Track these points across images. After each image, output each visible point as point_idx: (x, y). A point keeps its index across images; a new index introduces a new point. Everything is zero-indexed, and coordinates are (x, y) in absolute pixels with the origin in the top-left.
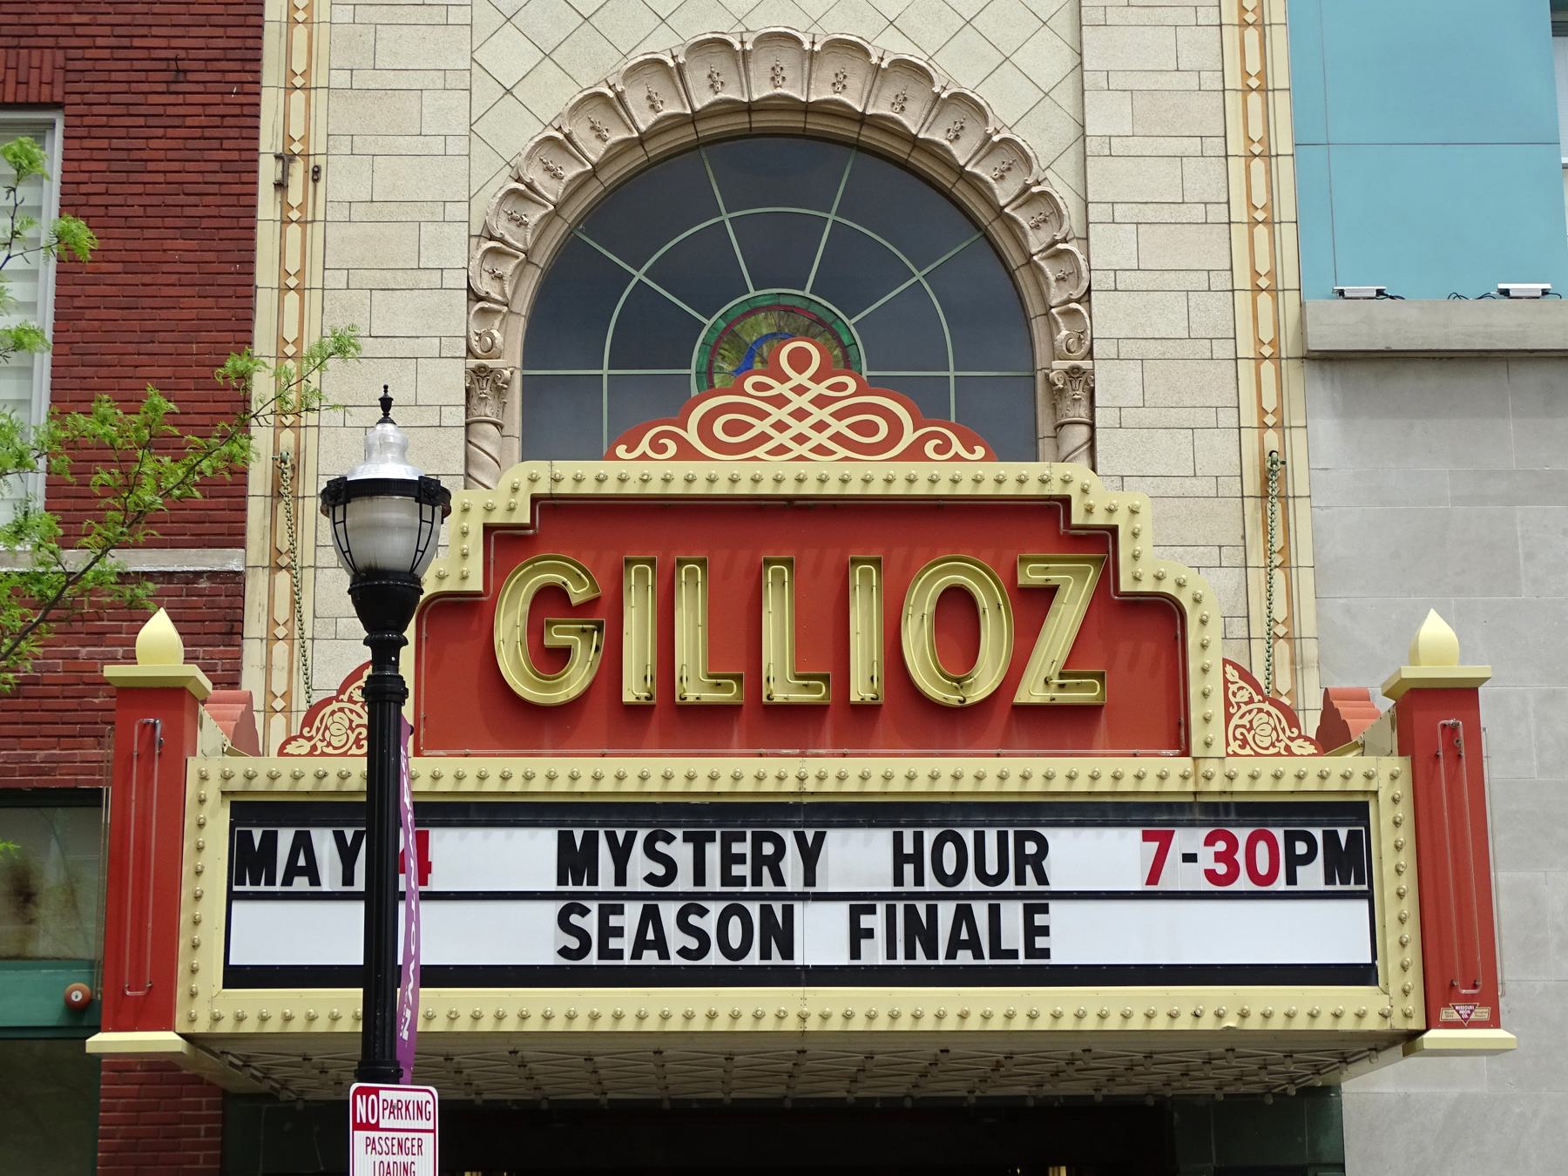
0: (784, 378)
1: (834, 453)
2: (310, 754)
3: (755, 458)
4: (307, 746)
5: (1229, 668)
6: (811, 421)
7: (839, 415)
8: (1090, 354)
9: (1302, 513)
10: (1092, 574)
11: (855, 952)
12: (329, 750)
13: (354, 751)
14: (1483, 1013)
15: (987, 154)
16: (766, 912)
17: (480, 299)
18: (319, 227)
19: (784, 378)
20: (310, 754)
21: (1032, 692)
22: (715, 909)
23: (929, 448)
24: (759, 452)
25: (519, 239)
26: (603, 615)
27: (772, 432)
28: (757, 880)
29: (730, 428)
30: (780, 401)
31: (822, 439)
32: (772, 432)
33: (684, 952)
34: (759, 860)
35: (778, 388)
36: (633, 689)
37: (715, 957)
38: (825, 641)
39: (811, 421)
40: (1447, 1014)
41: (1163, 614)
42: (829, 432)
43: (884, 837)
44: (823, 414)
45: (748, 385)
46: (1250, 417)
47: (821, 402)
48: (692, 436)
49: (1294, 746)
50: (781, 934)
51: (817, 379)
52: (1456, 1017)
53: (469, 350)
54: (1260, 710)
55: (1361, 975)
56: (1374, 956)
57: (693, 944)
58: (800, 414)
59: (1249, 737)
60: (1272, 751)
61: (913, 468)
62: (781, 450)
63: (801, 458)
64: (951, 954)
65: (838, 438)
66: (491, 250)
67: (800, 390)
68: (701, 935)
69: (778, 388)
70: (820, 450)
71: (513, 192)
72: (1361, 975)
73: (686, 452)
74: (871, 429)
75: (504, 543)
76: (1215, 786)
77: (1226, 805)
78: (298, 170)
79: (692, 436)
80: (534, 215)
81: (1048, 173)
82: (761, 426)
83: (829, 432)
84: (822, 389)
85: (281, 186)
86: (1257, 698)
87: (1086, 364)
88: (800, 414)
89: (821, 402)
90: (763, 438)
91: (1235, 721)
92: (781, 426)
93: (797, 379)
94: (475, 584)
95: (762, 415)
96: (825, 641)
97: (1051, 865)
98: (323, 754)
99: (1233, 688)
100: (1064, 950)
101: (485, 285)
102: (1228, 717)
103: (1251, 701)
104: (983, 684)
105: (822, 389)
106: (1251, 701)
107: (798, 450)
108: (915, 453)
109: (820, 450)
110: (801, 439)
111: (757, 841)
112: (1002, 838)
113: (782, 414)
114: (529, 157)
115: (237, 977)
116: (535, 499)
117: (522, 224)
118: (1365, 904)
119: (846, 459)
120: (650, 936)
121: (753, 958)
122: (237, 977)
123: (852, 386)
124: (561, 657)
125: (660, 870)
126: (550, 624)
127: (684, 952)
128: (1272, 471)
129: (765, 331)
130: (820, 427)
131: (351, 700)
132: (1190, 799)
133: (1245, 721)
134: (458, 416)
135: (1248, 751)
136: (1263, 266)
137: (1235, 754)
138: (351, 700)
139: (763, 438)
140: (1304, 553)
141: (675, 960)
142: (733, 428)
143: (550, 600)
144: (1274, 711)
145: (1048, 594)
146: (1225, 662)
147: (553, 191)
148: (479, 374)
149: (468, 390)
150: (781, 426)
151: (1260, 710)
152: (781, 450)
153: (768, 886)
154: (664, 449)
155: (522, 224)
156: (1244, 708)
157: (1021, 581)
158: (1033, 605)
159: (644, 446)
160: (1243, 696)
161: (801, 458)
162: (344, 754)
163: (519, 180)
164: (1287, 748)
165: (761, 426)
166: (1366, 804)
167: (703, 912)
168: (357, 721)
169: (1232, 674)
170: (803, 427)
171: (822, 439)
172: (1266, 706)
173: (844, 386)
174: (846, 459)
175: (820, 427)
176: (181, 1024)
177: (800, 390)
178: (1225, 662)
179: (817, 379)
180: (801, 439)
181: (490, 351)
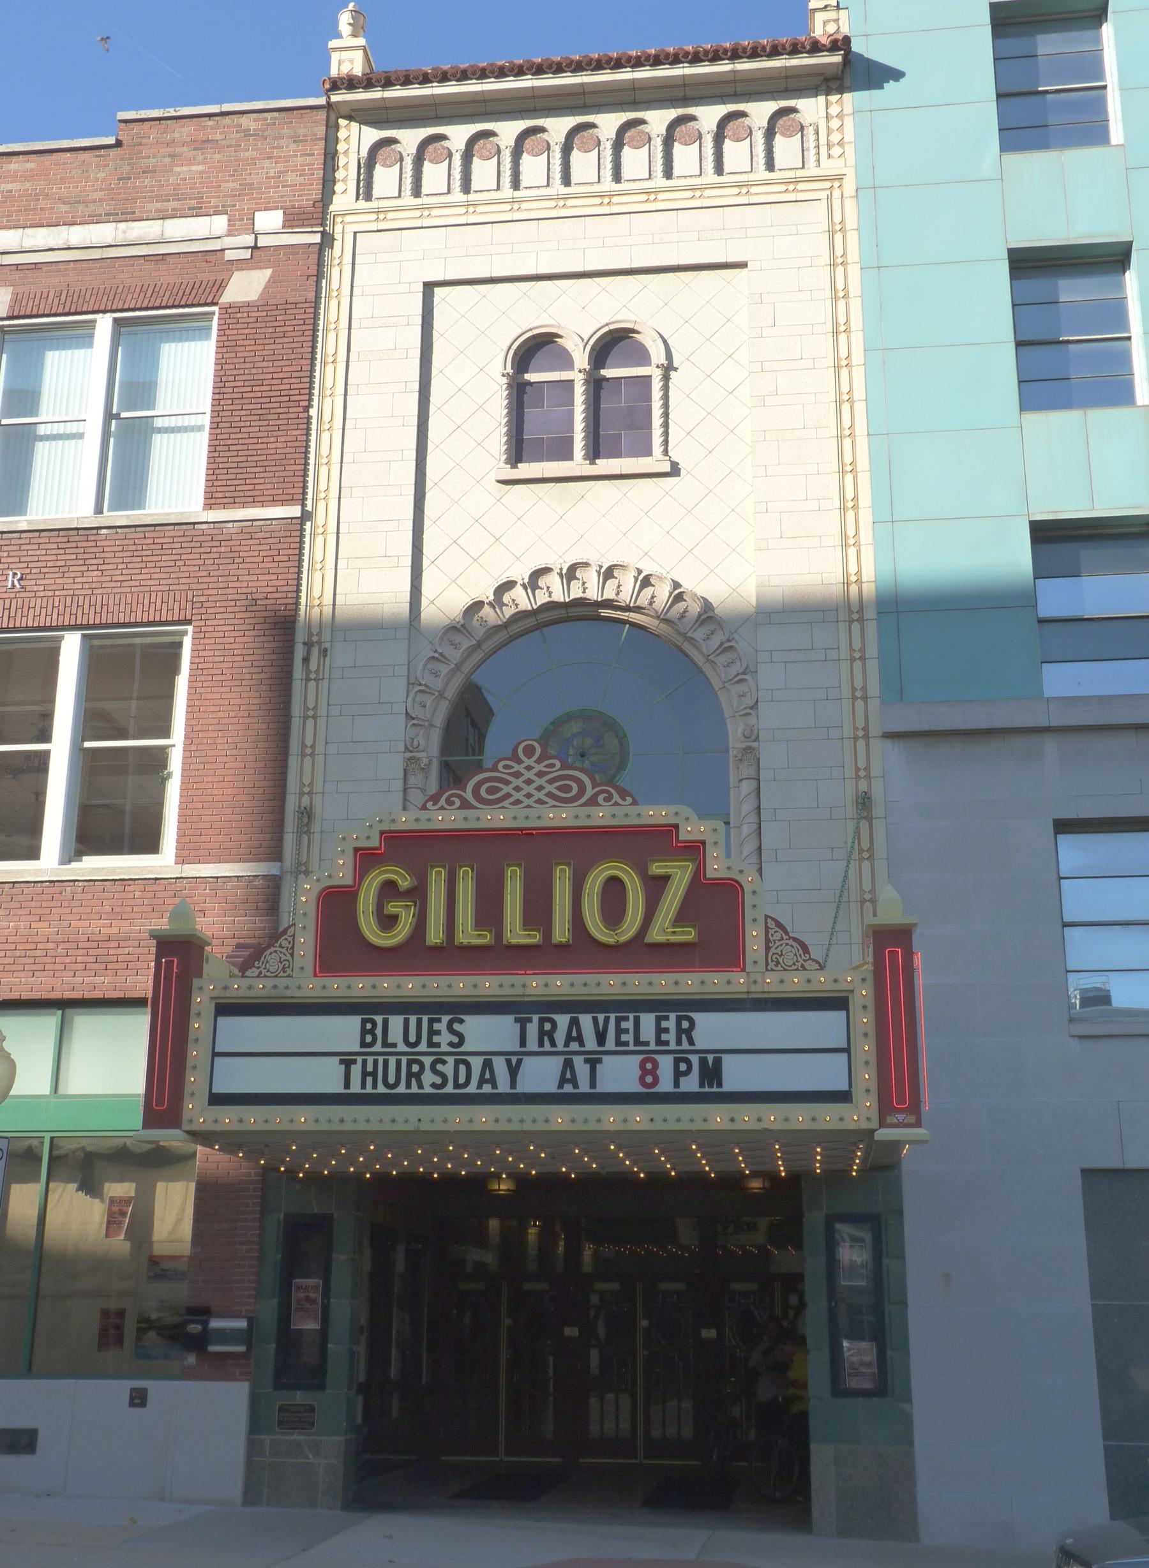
0: (520, 762)
1: (546, 803)
2: (258, 976)
3: (503, 807)
4: (257, 972)
5: (769, 920)
6: (535, 785)
7: (550, 782)
8: (757, 738)
9: (880, 827)
10: (691, 867)
11: (677, 1084)
12: (269, 974)
13: (282, 974)
14: (912, 1119)
15: (700, 625)
16: (703, 1062)
17: (413, 719)
18: (326, 682)
19: (520, 762)
20: (258, 976)
21: (656, 935)
22: (451, 1060)
23: (600, 799)
24: (506, 803)
25: (438, 683)
26: (418, 894)
27: (513, 792)
28: (679, 1042)
29: (490, 791)
30: (517, 775)
31: (541, 795)
32: (513, 792)
33: (433, 1085)
34: (680, 1031)
35: (517, 768)
36: (435, 935)
37: (449, 1089)
38: (537, 910)
39: (535, 785)
40: (889, 1120)
41: (730, 889)
43: (355, 1021)
44: (542, 782)
45: (500, 766)
46: (850, 772)
47: (540, 774)
48: (468, 795)
49: (806, 965)
50: (712, 1073)
51: (538, 761)
52: (895, 1121)
53: (406, 748)
54: (787, 944)
55: (844, 1097)
56: (850, 1086)
57: (439, 1081)
58: (529, 782)
59: (781, 960)
60: (794, 967)
61: (591, 810)
62: (517, 802)
63: (529, 806)
64: (480, 1086)
65: (550, 795)
66: (420, 691)
67: (529, 768)
68: (443, 1076)
69: (517, 768)
70: (540, 802)
71: (433, 658)
72: (844, 1097)
73: (465, 805)
74: (568, 789)
75: (366, 859)
76: (758, 988)
77: (766, 999)
78: (315, 651)
79: (468, 795)
80: (444, 669)
81: (736, 636)
82: (507, 789)
83: (545, 791)
84: (539, 768)
85: (306, 660)
86: (785, 937)
87: (755, 745)
88: (529, 782)
89: (540, 774)
90: (508, 795)
91: (773, 951)
92: (518, 789)
93: (528, 762)
94: (348, 881)
95: (507, 783)
96: (537, 910)
97: (695, 1034)
98: (265, 976)
99: (771, 932)
100: (731, 1082)
101: (416, 711)
102: (768, 949)
103: (782, 939)
104: (629, 929)
105: (539, 768)
106: (782, 939)
107: (527, 802)
108: (593, 802)
109: (540, 802)
110: (529, 796)
111: (679, 1020)
112: (419, 1023)
113: (518, 782)
114: (442, 639)
115: (216, 1099)
116: (382, 833)
117: (436, 675)
118: (845, 1055)
119: (554, 806)
120: (487, 1076)
121: (401, 1089)
122: (216, 1099)
123: (558, 764)
124: (394, 919)
125: (456, 1040)
126: (388, 902)
127: (433, 1085)
128: (864, 802)
129: (575, 731)
130: (540, 788)
131: (281, 946)
132: (745, 996)
133: (778, 951)
134: (398, 785)
135: (780, 968)
136: (858, 684)
137: (772, 970)
138: (281, 946)
139: (508, 795)
140: (881, 850)
141: (428, 1090)
142: (490, 791)
143: (389, 889)
144: (795, 945)
145: (665, 879)
146: (767, 917)
147: (455, 655)
148: (413, 760)
149: (405, 770)
150: (518, 789)
151: (787, 944)
152: (517, 802)
153: (685, 1045)
154: (453, 803)
155: (436, 675)
156: (778, 943)
157: (650, 873)
158: (656, 886)
159: (442, 802)
160: (777, 936)
161: (529, 806)
162: (276, 976)
163: (436, 651)
164: (803, 966)
165: (507, 789)
166: (847, 998)
167: (444, 1062)
168: (284, 958)
169: (771, 924)
170: (530, 789)
171: (541, 795)
172: (791, 942)
173: (553, 765)
174: (554, 806)
175: (540, 788)
176: (186, 1126)
177: (529, 768)
178: (767, 917)
179: (538, 761)
180: (529, 796)
181: (417, 749)
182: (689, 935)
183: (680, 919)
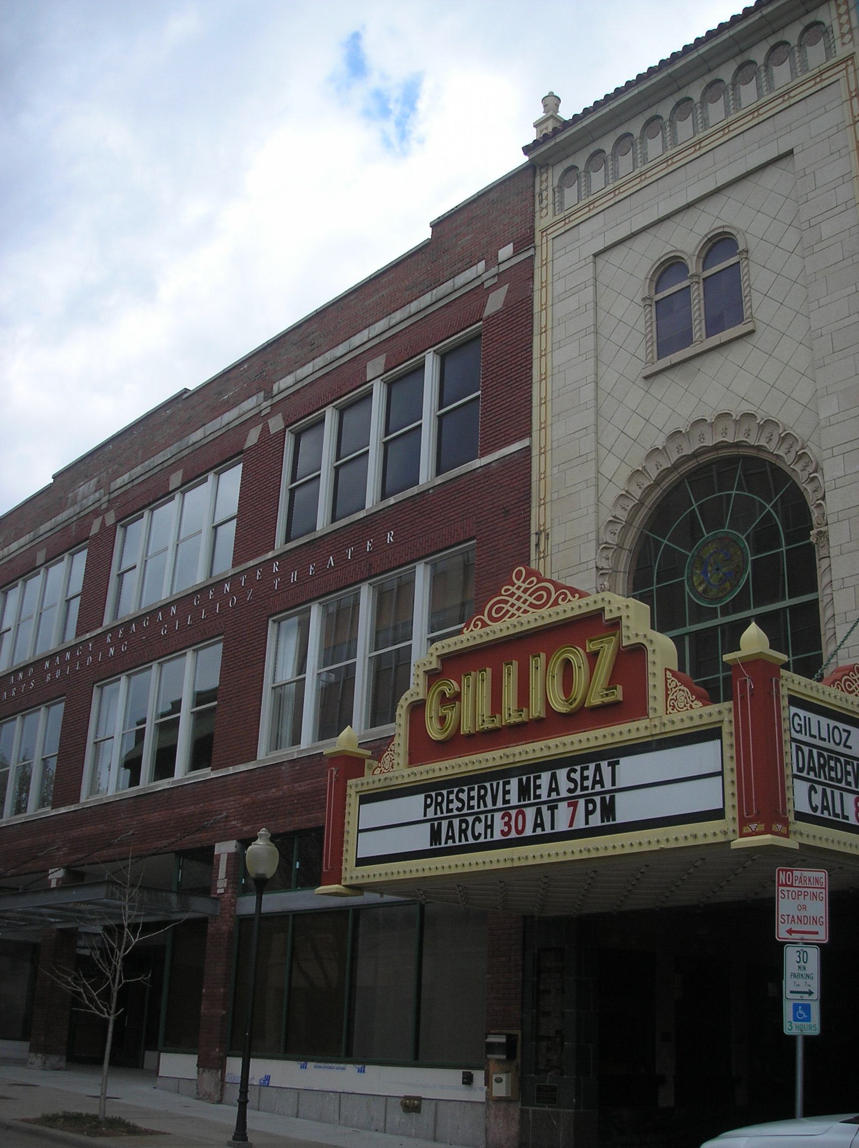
7: (530, 595)
18: (549, 557)
19: (513, 584)
35: (513, 589)
40: (746, 830)
42: (509, 604)
51: (524, 582)
66: (604, 548)
67: (519, 588)
69: (513, 589)
72: (717, 814)
73: (484, 625)
74: (539, 598)
78: (543, 536)
84: (525, 585)
85: (537, 545)
86: (679, 684)
91: (670, 697)
93: (519, 583)
99: (669, 681)
101: (603, 564)
102: (667, 695)
123: (534, 579)
146: (666, 669)
156: (674, 690)
159: (472, 627)
164: (691, 706)
169: (669, 674)
173: (533, 581)
176: (343, 883)
178: (666, 669)
179: (524, 582)
182: (618, 694)
183: (611, 685)
